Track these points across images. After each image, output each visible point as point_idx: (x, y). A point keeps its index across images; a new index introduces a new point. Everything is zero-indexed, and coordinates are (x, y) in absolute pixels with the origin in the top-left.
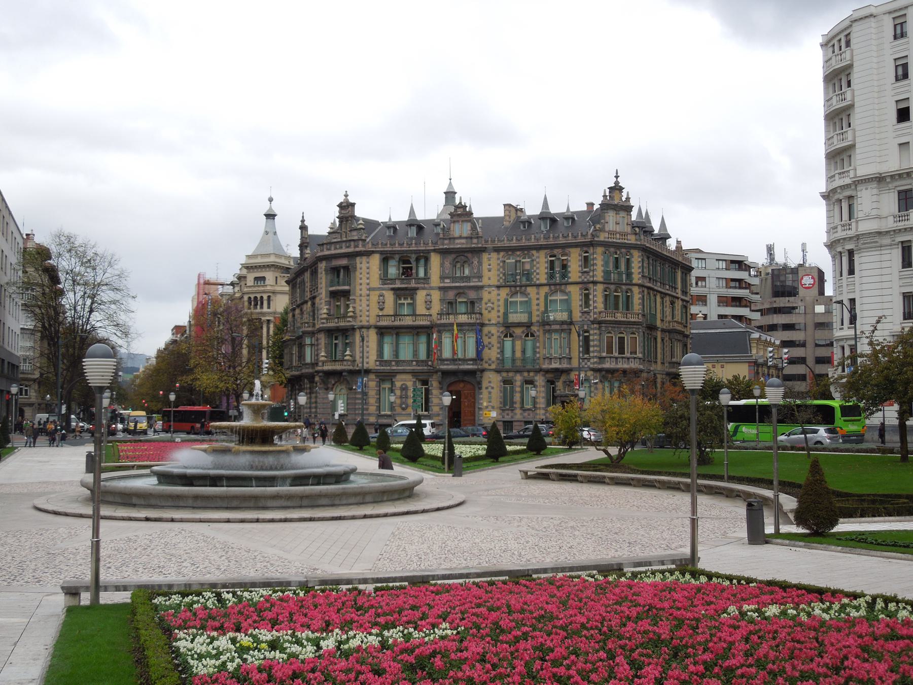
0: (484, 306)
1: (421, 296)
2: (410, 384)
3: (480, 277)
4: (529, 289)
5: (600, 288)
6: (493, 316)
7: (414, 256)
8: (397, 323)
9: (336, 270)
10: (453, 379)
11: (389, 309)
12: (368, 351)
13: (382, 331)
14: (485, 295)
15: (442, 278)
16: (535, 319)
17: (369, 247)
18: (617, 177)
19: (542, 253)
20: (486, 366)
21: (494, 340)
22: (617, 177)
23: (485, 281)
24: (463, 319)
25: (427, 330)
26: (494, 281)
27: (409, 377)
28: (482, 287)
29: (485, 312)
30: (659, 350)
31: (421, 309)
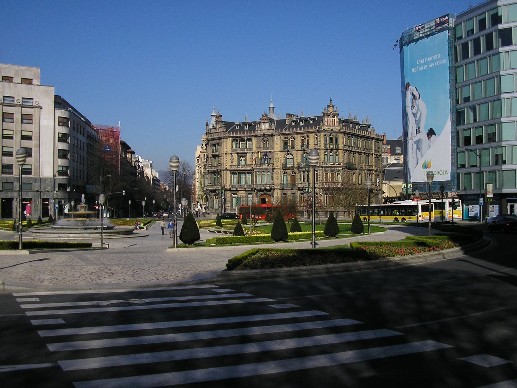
0: (275, 160)
1: (249, 156)
2: (244, 195)
3: (273, 148)
4: (293, 153)
5: (322, 151)
6: (278, 165)
7: (245, 138)
8: (238, 169)
9: (215, 145)
10: (262, 193)
11: (235, 163)
12: (227, 180)
13: (233, 173)
14: (276, 156)
15: (257, 148)
16: (296, 166)
17: (227, 135)
18: (331, 101)
19: (299, 136)
20: (275, 187)
21: (279, 175)
22: (331, 101)
23: (276, 149)
24: (266, 166)
25: (250, 172)
26: (279, 149)
27: (244, 192)
28: (274, 152)
29: (275, 163)
30: (360, 180)
31: (249, 163)
